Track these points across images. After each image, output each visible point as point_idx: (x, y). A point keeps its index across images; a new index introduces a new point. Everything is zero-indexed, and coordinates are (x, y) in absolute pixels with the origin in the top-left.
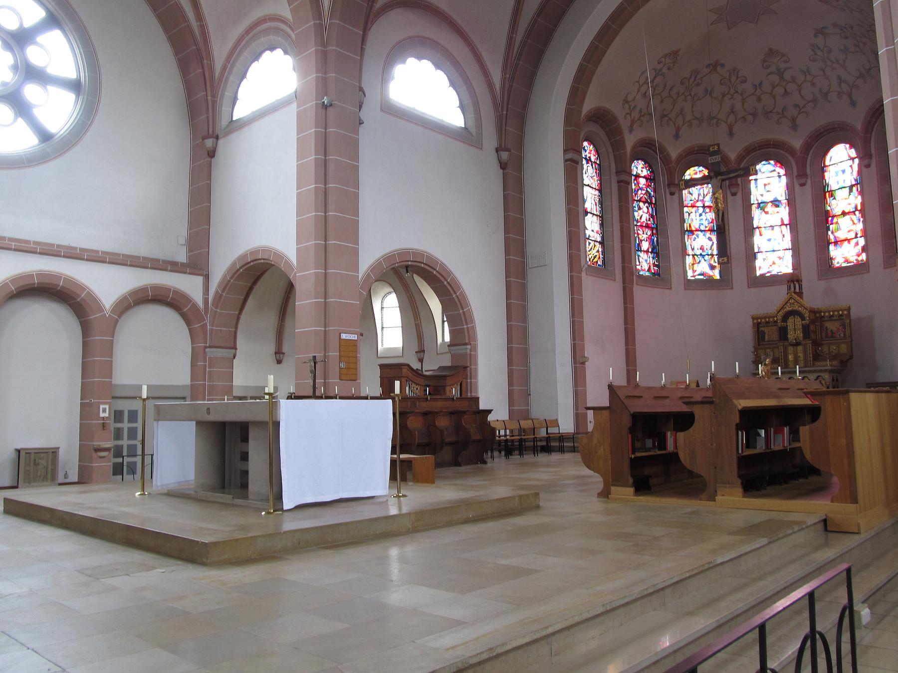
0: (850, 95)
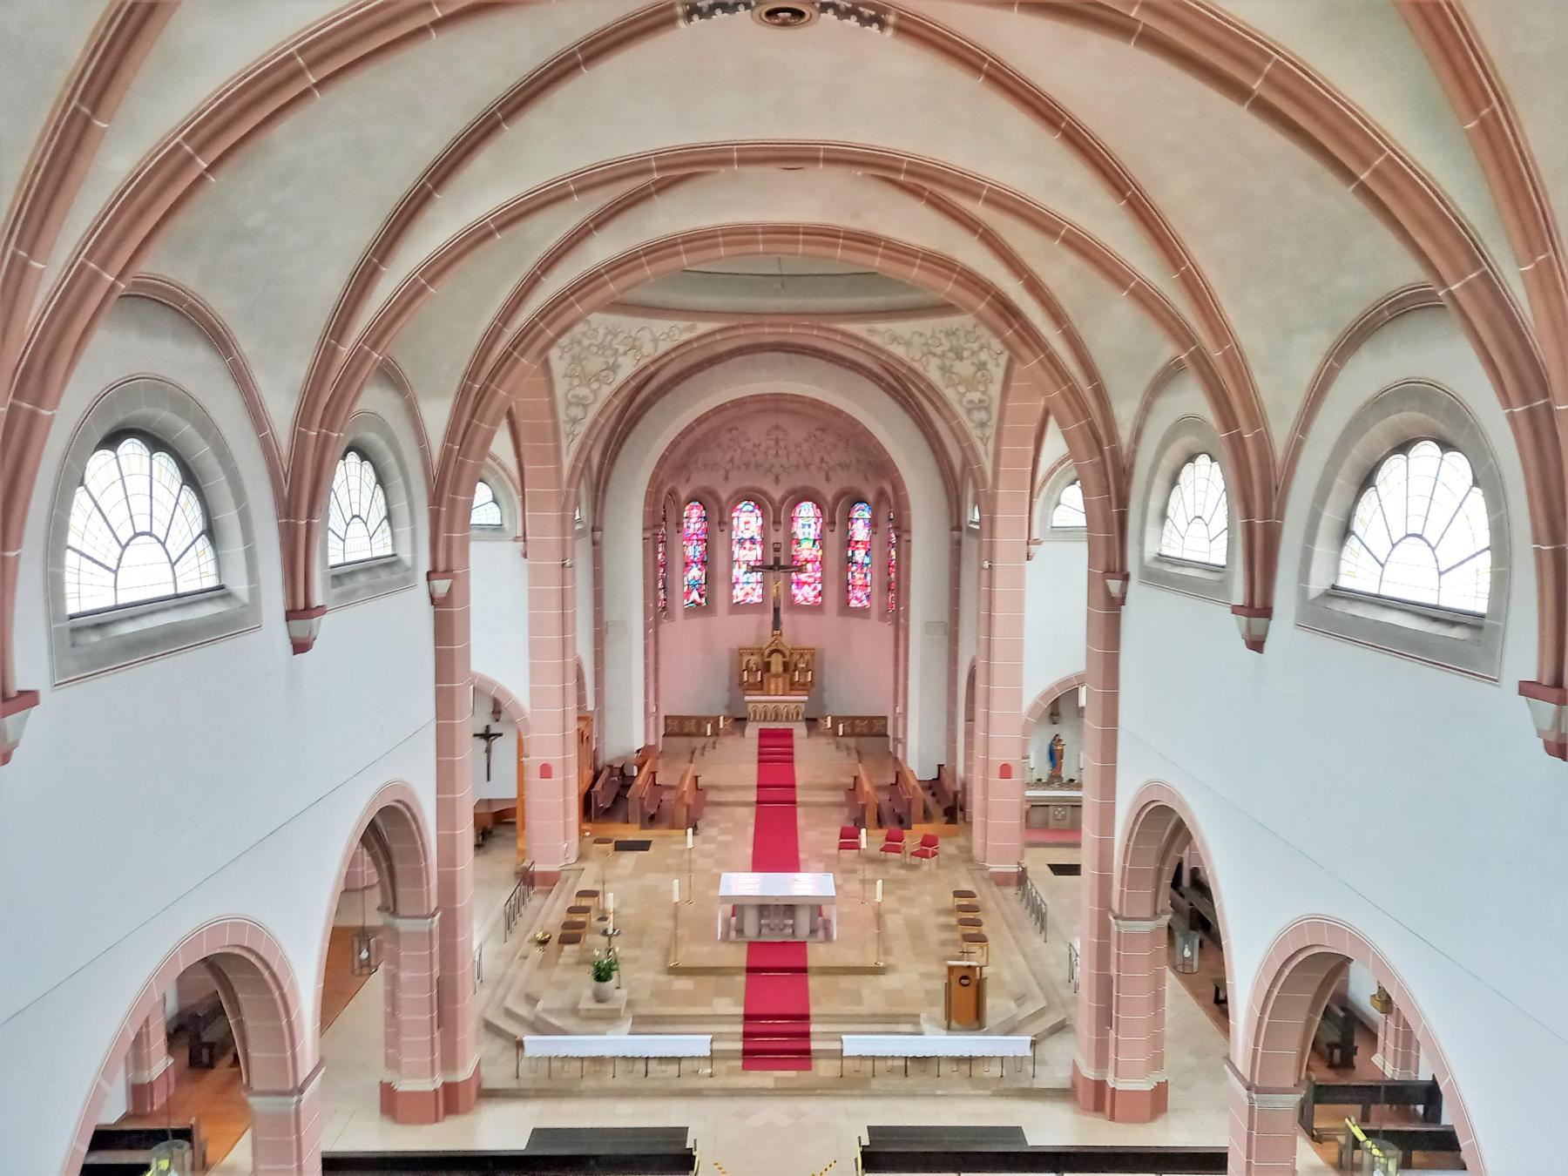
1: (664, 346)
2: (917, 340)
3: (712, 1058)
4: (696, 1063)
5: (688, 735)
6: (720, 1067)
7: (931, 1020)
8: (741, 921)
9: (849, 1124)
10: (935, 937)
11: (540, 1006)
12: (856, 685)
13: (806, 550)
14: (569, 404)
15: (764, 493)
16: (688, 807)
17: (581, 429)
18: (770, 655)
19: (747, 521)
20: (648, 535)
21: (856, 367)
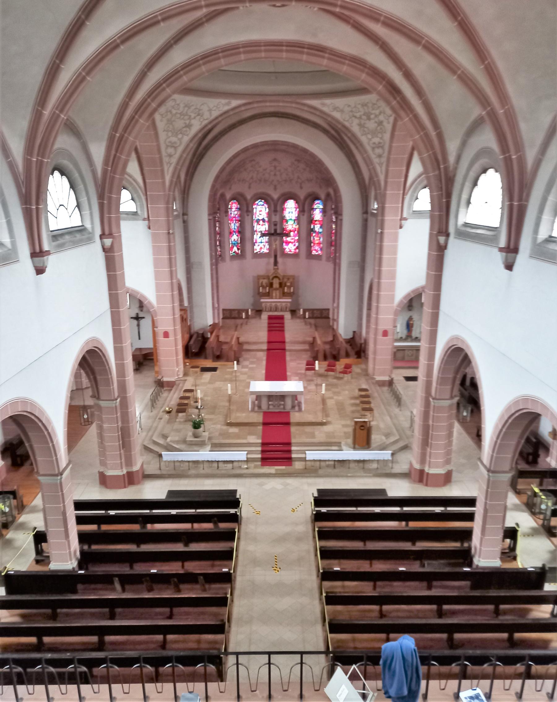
0: (301, 184)
1: (215, 114)
2: (347, 109)
3: (248, 461)
4: (240, 463)
5: (234, 318)
6: (252, 465)
7: (347, 444)
8: (260, 402)
9: (309, 488)
10: (349, 409)
11: (169, 439)
12: (314, 295)
13: (291, 225)
14: (167, 146)
15: (269, 195)
16: (235, 352)
17: (174, 160)
18: (273, 279)
19: (261, 210)
20: (211, 217)
21: (315, 125)
